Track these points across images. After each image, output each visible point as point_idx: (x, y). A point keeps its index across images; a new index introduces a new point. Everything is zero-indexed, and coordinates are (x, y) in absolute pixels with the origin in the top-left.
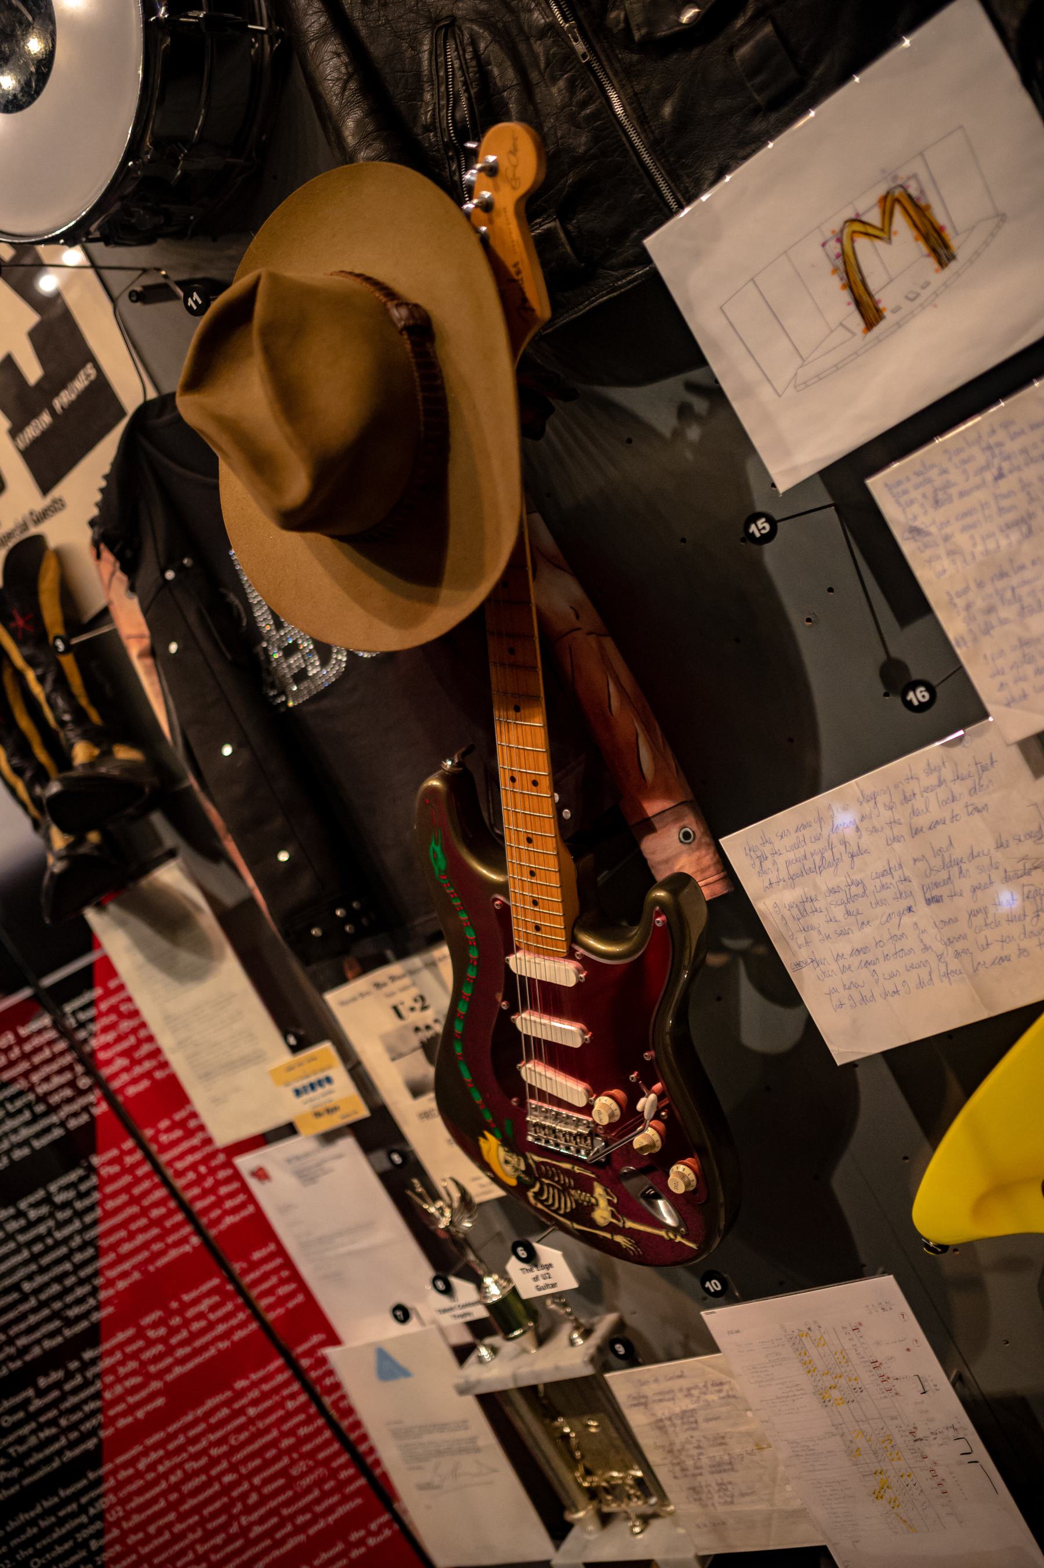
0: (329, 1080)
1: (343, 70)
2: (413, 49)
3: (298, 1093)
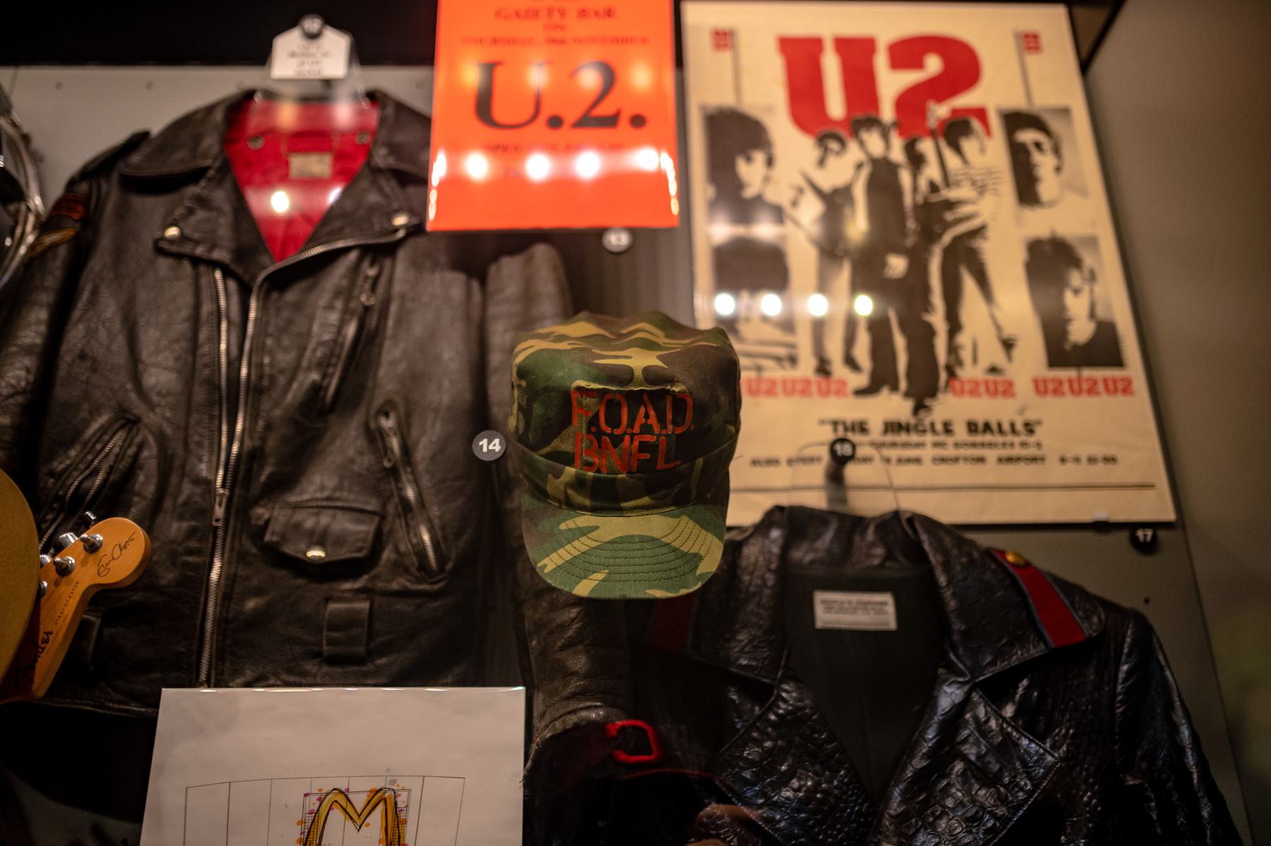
1: (23, 384)
2: (91, 413)
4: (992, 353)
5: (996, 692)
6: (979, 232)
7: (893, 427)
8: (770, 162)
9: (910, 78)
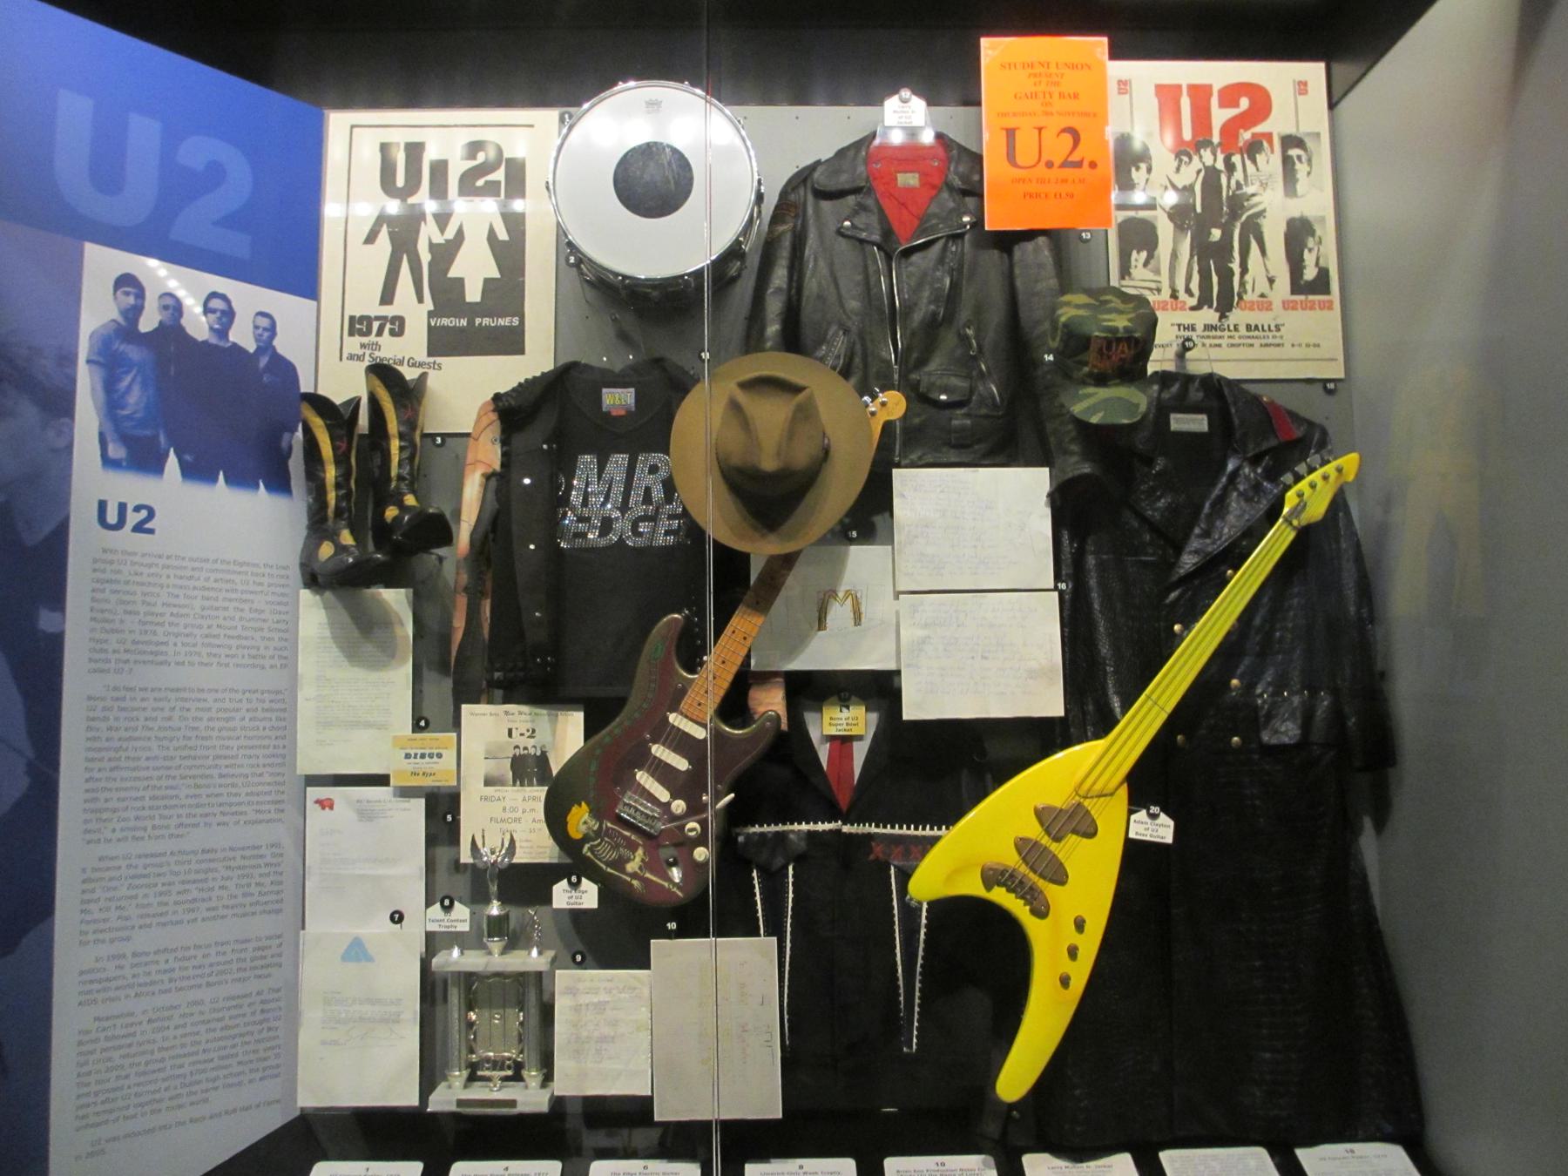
0: (440, 756)
3: (408, 756)
4: (1262, 285)
5: (1255, 461)
6: (1261, 214)
7: (1208, 327)
8: (1149, 170)
9: (1231, 112)
